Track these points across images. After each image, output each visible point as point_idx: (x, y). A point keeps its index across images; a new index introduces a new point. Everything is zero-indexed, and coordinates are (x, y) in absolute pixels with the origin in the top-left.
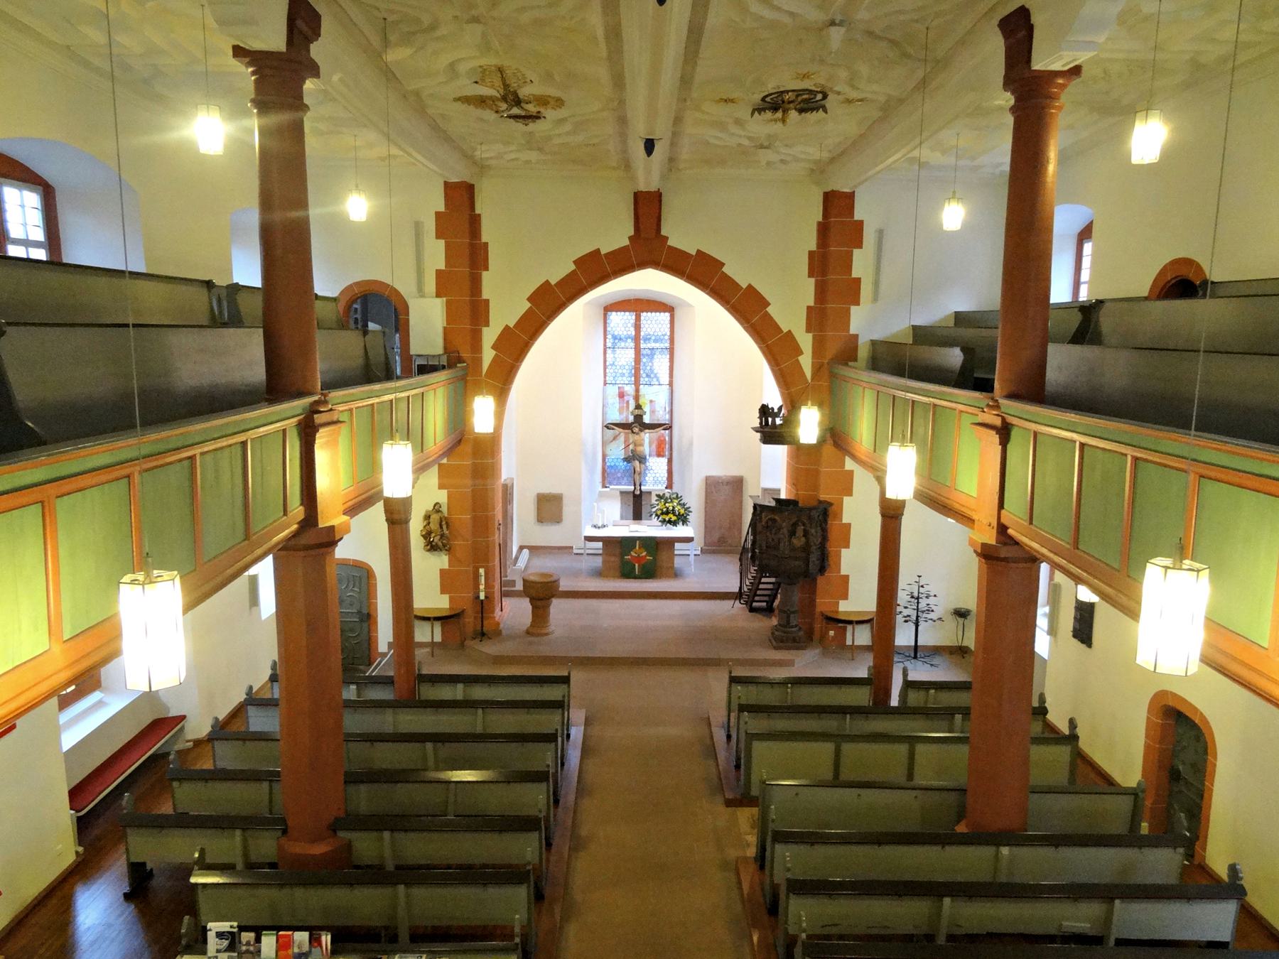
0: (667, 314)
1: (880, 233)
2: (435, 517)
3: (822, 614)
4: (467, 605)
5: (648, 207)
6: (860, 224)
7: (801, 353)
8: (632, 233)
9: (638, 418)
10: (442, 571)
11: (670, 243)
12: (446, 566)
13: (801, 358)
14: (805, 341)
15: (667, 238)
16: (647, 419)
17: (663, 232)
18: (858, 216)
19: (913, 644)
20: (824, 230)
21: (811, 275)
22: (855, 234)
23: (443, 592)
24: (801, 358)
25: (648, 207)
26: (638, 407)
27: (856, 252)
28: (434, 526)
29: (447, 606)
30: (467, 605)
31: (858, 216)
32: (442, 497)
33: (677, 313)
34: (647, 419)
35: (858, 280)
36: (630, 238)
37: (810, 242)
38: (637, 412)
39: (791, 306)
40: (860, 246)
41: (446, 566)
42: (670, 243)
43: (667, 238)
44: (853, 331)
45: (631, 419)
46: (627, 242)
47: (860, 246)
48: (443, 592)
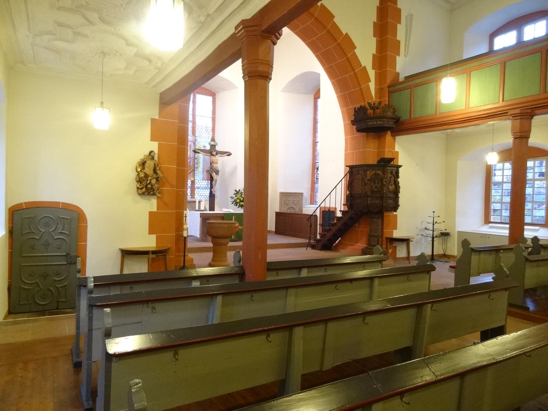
0: (210, 99)
1: (410, 17)
2: (150, 164)
3: (387, 238)
4: (170, 244)
6: (399, 10)
7: (370, 81)
9: (213, 147)
10: (151, 214)
12: (155, 209)
13: (370, 84)
14: (372, 74)
16: (218, 148)
19: (431, 254)
21: (374, 36)
23: (151, 232)
24: (370, 84)
26: (213, 140)
28: (149, 170)
29: (155, 245)
30: (170, 244)
32: (154, 146)
33: (218, 97)
34: (218, 148)
37: (373, 17)
38: (212, 143)
39: (365, 51)
41: (155, 209)
44: (398, 70)
45: (208, 148)
48: (151, 232)
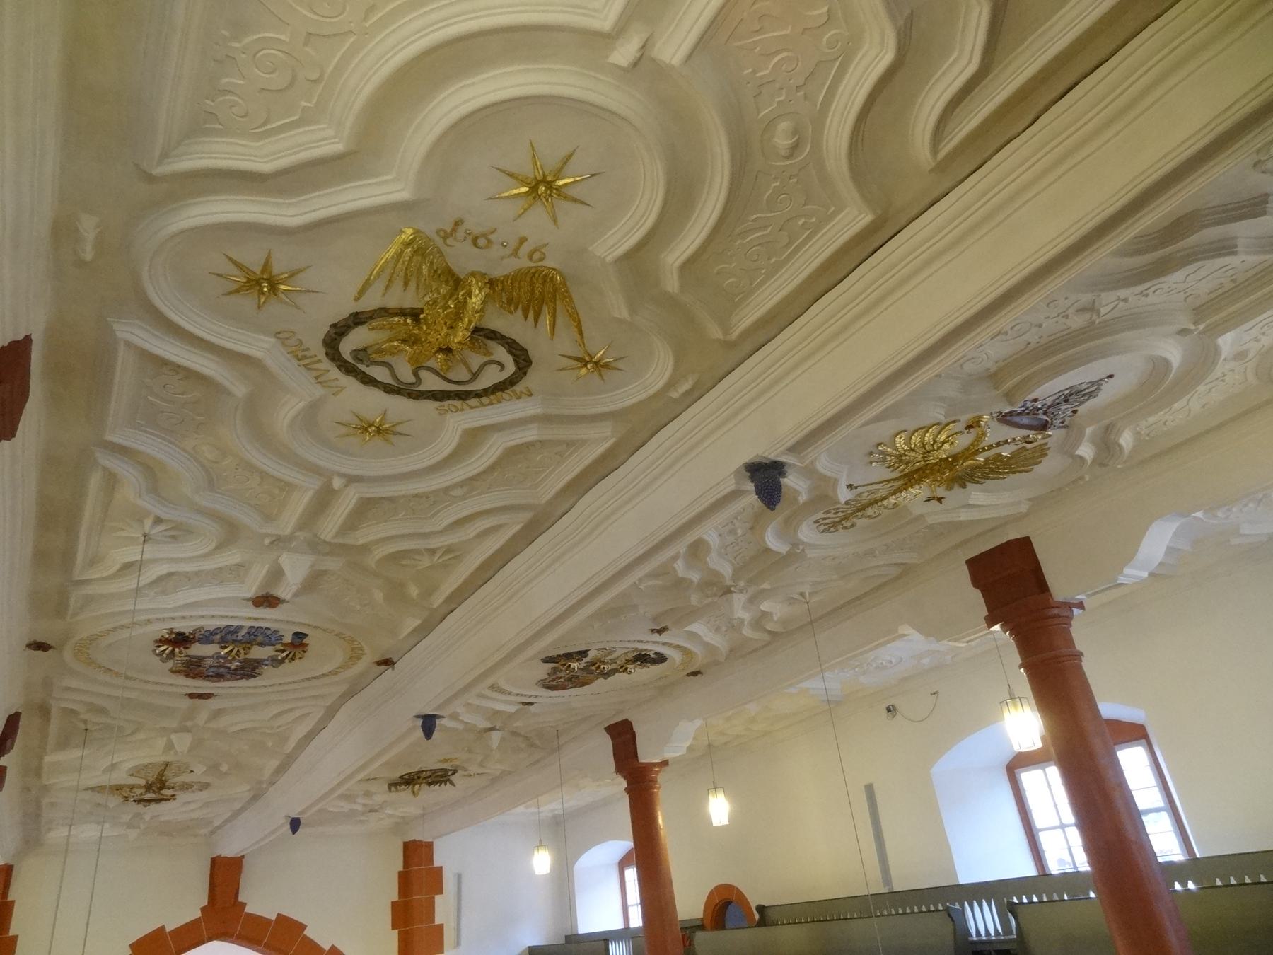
1: (459, 877)
5: (225, 875)
8: (205, 903)
11: (247, 910)
15: (244, 905)
17: (241, 899)
18: (437, 863)
20: (405, 880)
22: (435, 880)
25: (225, 875)
27: (438, 898)
31: (437, 863)
35: (441, 927)
36: (203, 910)
40: (441, 892)
42: (247, 910)
43: (244, 905)
46: (198, 914)
47: (441, 892)
